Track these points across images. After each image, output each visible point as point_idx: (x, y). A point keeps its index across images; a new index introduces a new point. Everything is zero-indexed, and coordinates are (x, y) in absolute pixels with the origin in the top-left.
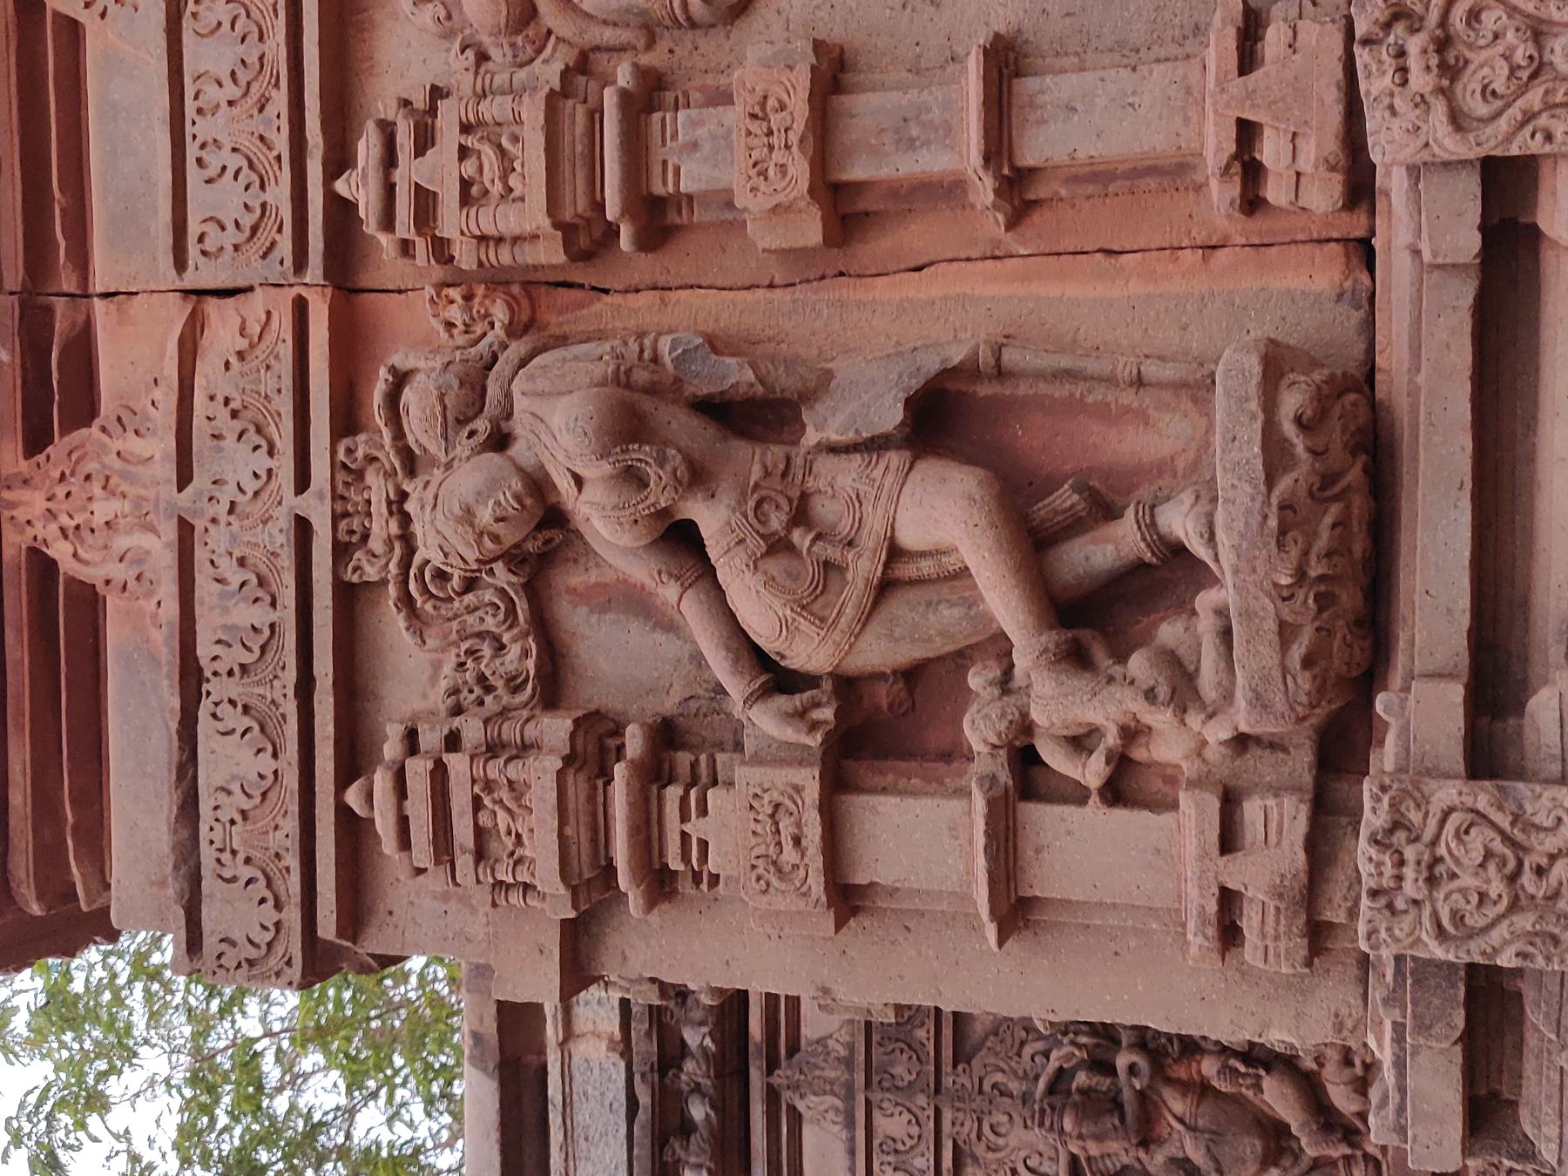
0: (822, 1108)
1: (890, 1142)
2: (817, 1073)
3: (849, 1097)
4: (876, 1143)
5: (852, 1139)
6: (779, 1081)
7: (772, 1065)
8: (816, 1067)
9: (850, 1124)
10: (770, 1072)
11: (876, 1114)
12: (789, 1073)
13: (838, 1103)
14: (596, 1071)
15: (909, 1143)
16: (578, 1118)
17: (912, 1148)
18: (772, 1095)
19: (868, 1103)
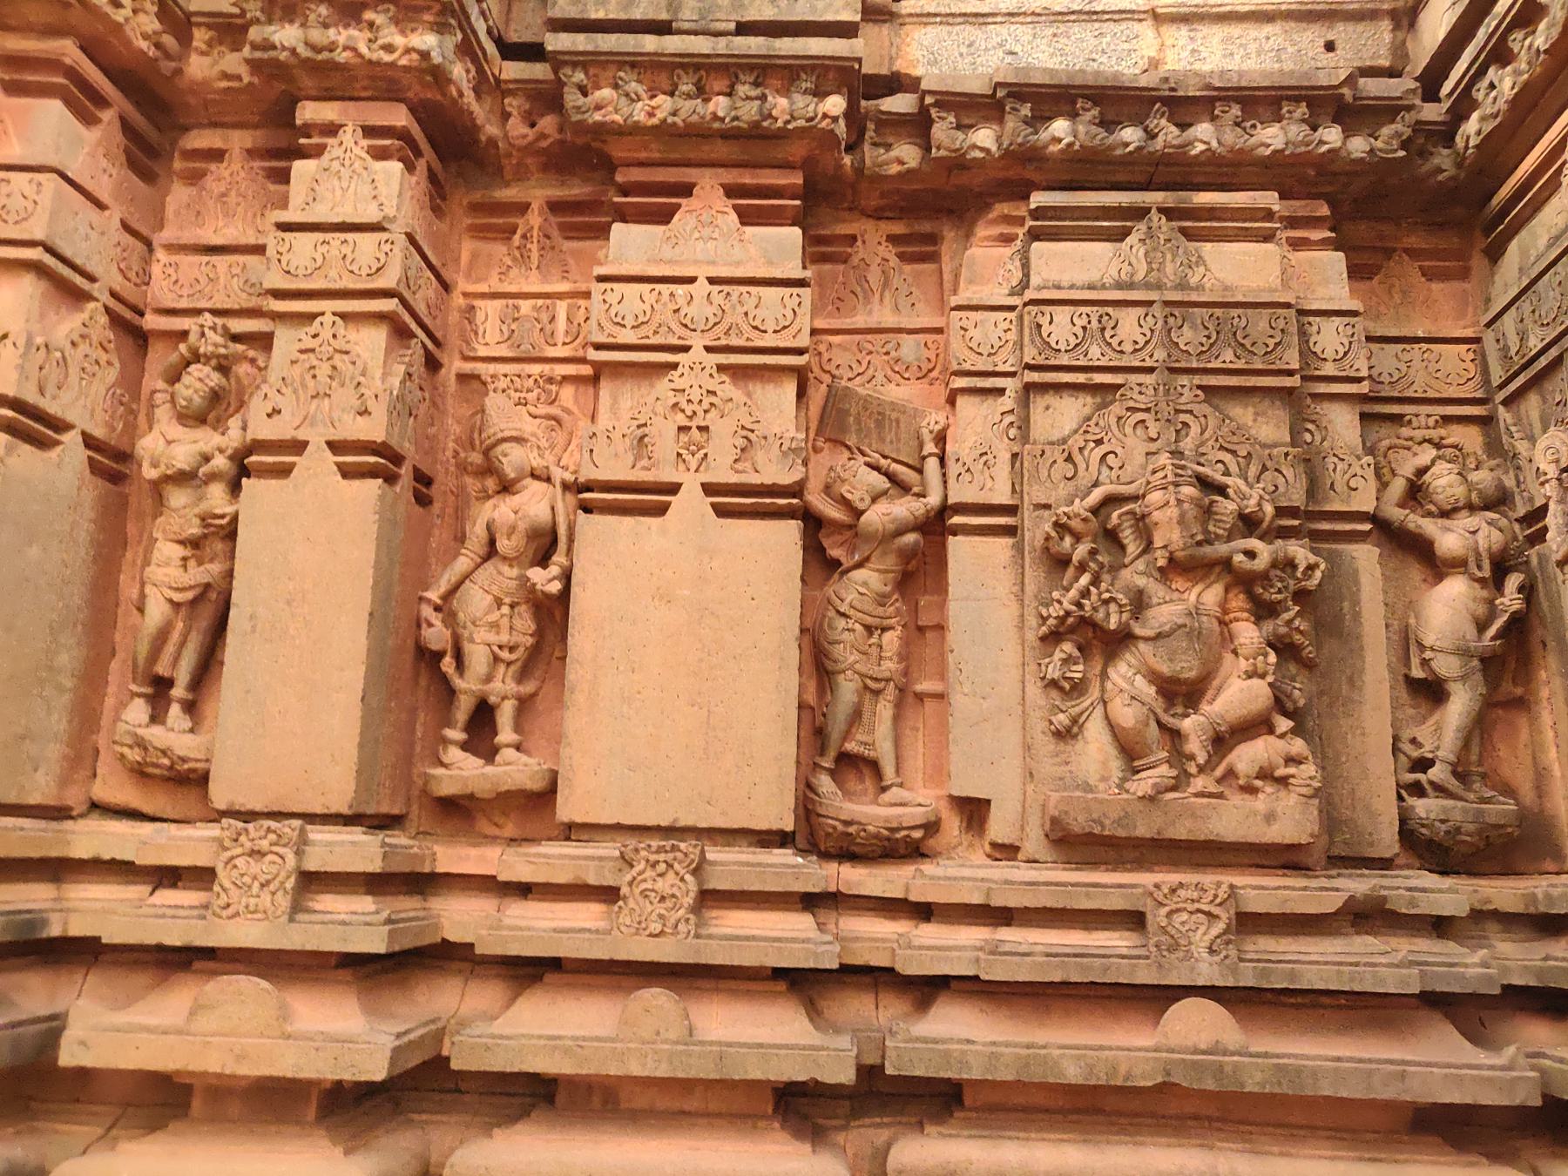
0: (1134, 261)
1: (1112, 323)
2: (1169, 256)
3: (1148, 286)
4: (1110, 310)
5: (1103, 287)
6: (1155, 219)
7: (1168, 213)
8: (1174, 256)
9: (1119, 286)
10: (1161, 210)
11: (1141, 311)
12: (1164, 229)
13: (1140, 276)
14: (1126, 46)
15: (1114, 342)
16: (1076, 28)
17: (1109, 344)
18: (1140, 213)
19: (1150, 303)
